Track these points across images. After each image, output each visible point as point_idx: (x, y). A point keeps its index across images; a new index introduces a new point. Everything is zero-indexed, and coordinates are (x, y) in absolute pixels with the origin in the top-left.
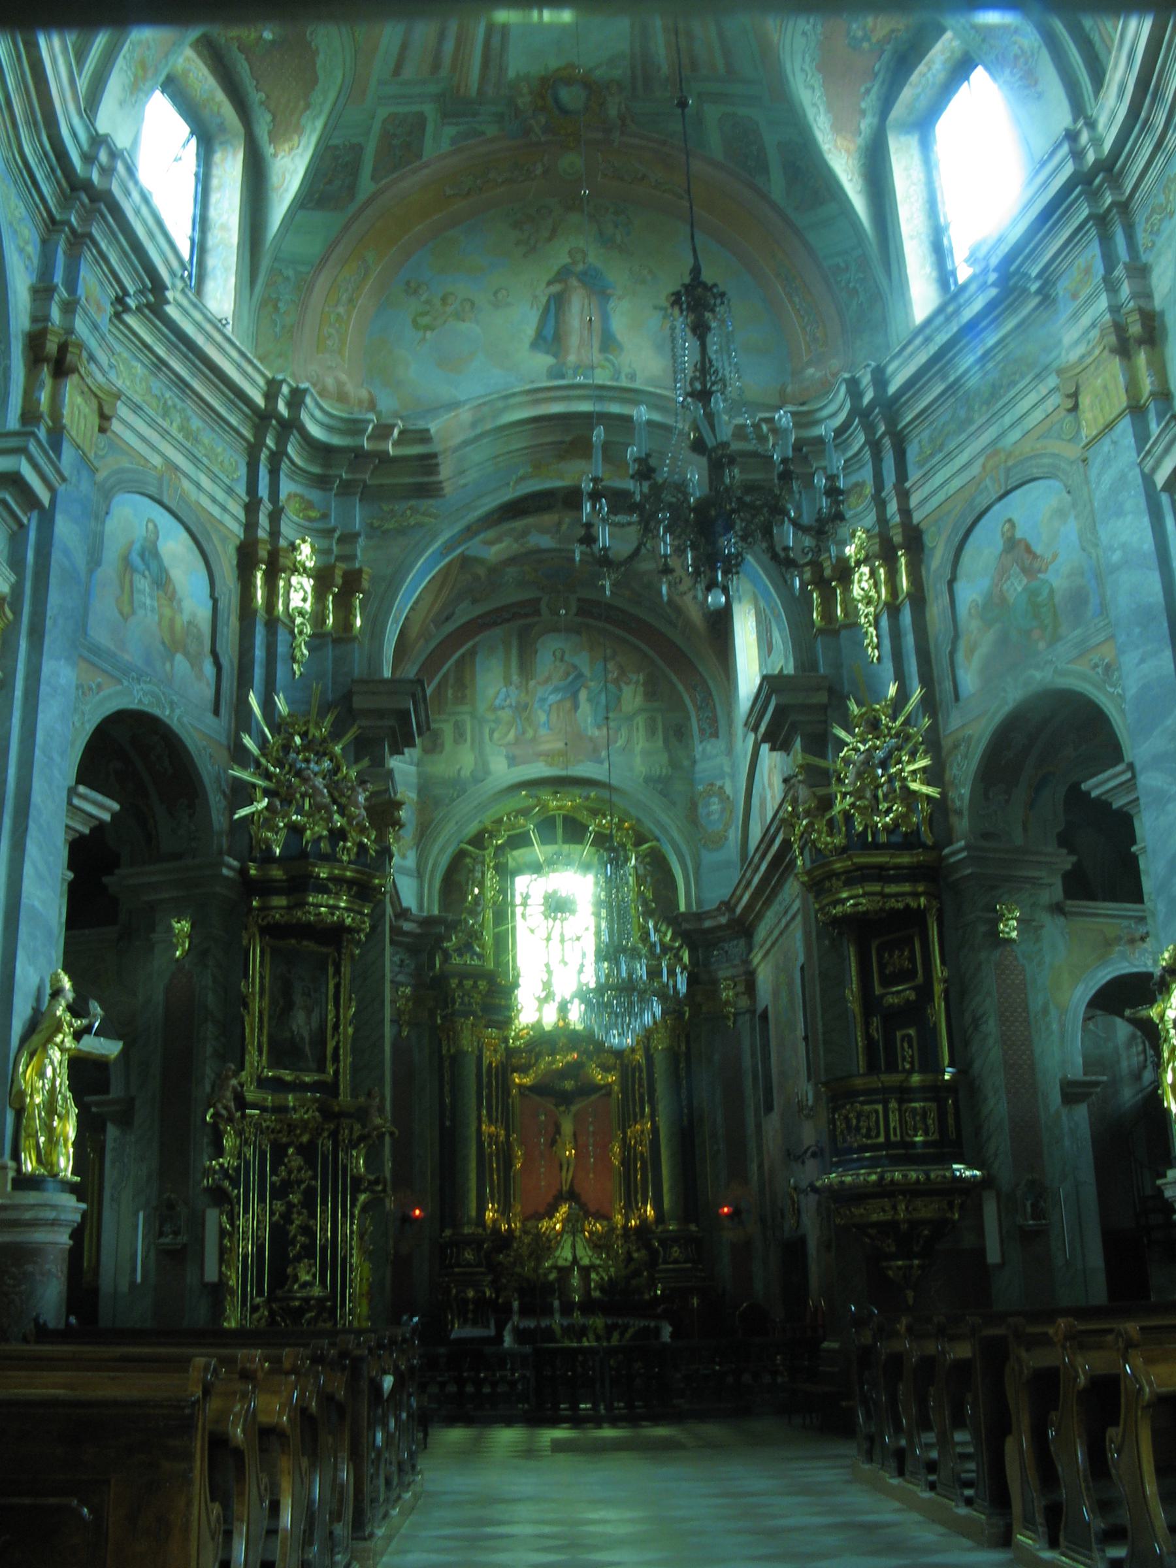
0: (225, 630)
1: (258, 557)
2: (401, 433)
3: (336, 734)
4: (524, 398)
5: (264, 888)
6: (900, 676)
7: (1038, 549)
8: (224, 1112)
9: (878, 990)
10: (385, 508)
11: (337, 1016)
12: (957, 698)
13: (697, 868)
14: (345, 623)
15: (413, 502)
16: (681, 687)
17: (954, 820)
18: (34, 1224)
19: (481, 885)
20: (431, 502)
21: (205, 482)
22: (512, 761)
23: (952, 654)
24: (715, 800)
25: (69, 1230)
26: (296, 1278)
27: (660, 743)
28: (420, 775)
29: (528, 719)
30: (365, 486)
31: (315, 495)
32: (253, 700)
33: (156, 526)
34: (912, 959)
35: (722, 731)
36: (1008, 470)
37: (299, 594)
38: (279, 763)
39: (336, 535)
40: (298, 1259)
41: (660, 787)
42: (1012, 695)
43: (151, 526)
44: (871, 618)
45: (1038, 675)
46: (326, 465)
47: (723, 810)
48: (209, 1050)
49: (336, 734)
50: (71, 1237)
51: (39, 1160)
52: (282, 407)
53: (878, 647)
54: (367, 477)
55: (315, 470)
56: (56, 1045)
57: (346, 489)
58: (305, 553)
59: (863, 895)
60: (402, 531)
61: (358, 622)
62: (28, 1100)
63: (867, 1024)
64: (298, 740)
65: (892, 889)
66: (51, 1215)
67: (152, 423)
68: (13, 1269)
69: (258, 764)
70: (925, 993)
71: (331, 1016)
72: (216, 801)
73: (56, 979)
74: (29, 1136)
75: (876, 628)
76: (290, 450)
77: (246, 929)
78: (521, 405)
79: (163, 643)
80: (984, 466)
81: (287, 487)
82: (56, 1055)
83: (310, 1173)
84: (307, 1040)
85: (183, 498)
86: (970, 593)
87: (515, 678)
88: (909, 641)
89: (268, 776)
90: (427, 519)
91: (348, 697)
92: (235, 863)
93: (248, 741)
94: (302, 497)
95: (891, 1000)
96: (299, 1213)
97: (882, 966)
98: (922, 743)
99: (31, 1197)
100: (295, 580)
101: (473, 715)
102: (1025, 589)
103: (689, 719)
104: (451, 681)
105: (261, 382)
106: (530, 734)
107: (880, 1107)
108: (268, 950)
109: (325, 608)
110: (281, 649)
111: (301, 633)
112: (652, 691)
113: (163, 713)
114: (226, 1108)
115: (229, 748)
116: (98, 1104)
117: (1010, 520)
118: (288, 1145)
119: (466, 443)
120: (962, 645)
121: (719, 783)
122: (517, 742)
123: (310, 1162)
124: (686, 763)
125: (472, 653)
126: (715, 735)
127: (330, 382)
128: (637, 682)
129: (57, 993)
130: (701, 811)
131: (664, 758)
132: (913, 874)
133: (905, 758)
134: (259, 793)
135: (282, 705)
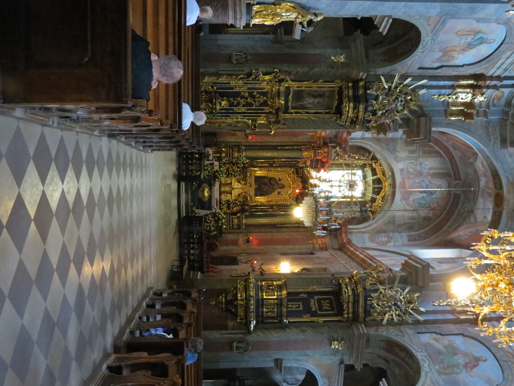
1: (479, 81)
5: (355, 88)
6: (427, 312)
7: (475, 370)
8: (278, 75)
9: (316, 298)
10: (498, 128)
11: (310, 113)
12: (419, 333)
13: (363, 232)
14: (452, 114)
15: (499, 138)
16: (426, 229)
17: (374, 328)
18: (235, 11)
19: (359, 159)
20: (499, 145)
22: (402, 170)
23: (436, 333)
24: (386, 239)
25: (233, 24)
26: (223, 101)
27: (407, 221)
28: (397, 138)
29: (417, 176)
30: (506, 120)
31: (503, 101)
32: (424, 81)
33: (492, 42)
34: (326, 310)
35: (410, 243)
36: (507, 362)
37: (464, 96)
38: (401, 92)
39: (487, 110)
40: (229, 101)
41: (392, 220)
42: (420, 355)
43: (492, 41)
44: (450, 303)
45: (426, 365)
47: (383, 242)
48: (299, 70)
49: (411, 111)
50: (231, 24)
51: (257, 12)
53: (439, 305)
56: (298, 16)
58: (480, 99)
59: (349, 295)
60: (488, 134)
61: (453, 119)
62: (278, 7)
63: (304, 293)
64: (409, 98)
65: (350, 305)
68: (219, 5)
69: (400, 84)
70: (314, 314)
71: (312, 111)
72: (386, 70)
73: (321, 14)
74: (265, 8)
75: (446, 305)
77: (341, 81)
79: (446, 48)
80: (508, 352)
81: (506, 91)
82: (294, 15)
83: (258, 105)
85: (504, 52)
86: (458, 341)
87: (431, 171)
88: (440, 317)
89: (396, 88)
90: (492, 143)
91: (424, 115)
92: (364, 77)
93: (409, 80)
94: (503, 96)
95: (312, 301)
96: (244, 101)
97: (324, 299)
98: (402, 319)
99: (244, 10)
101: (419, 157)
102: (459, 363)
103: (416, 231)
104: (431, 149)
106: (411, 176)
107: (275, 297)
108: (334, 89)
109: (459, 106)
110: (443, 91)
111: (449, 98)
112: (427, 219)
113: (420, 49)
114: (279, 76)
116: (281, 31)
117: (486, 360)
118: (267, 97)
120: (439, 337)
121: (392, 241)
122: (409, 172)
123: (261, 105)
124: (400, 230)
125: (441, 156)
126: (409, 240)
128: (429, 214)
129: (316, 15)
130: (383, 234)
131: (402, 222)
132: (355, 312)
133: (397, 312)
134: (390, 84)
135: (422, 92)
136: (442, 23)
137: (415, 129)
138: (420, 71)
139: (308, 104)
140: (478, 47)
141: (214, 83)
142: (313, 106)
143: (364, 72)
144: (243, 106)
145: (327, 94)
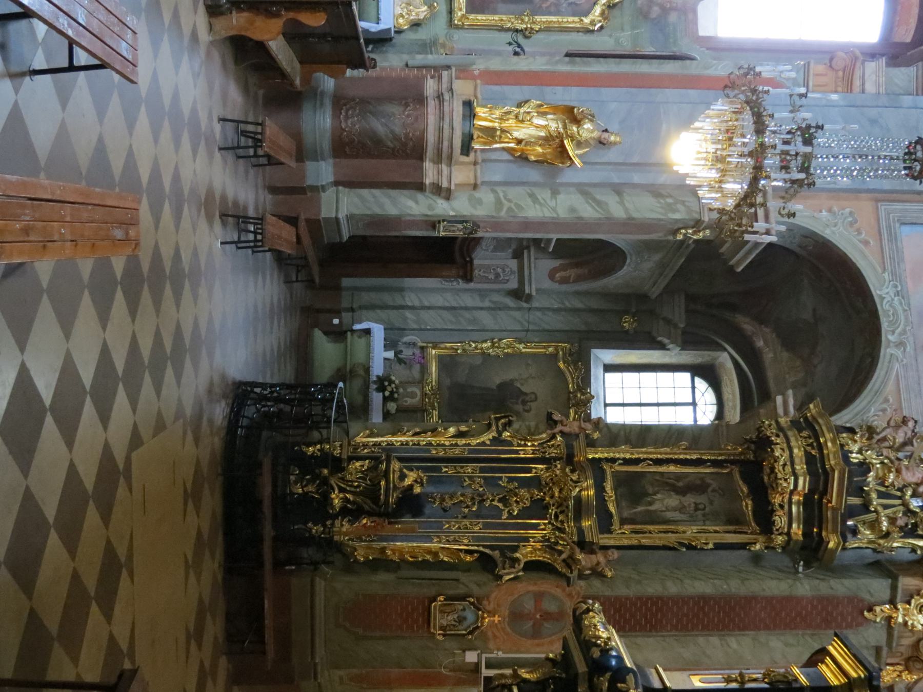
84: (651, 508)
113: (889, 336)
139: (667, 510)
142: (684, 517)
145: (714, 485)
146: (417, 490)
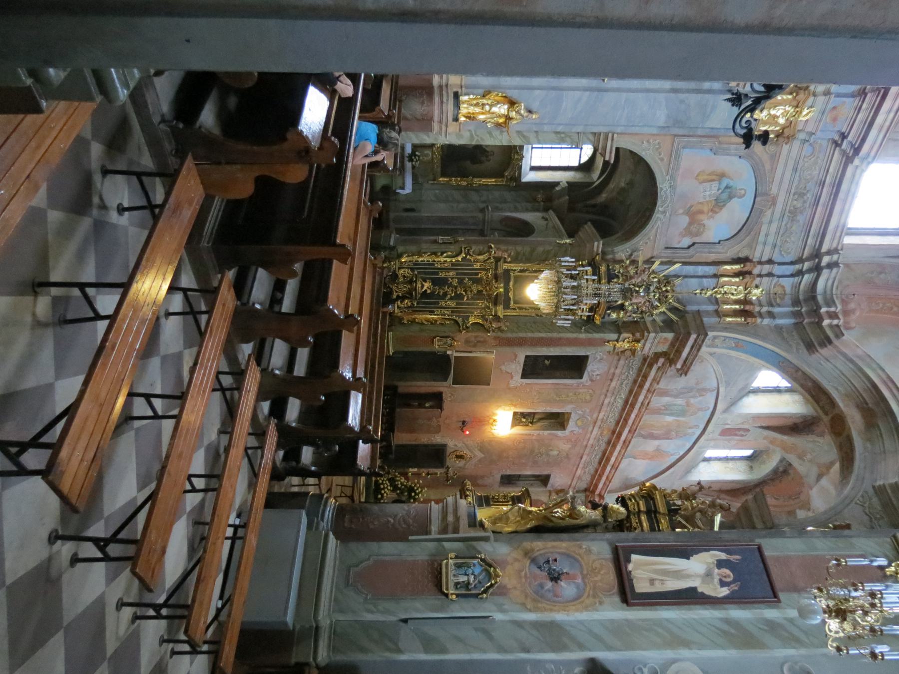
0: (706, 250)
1: (744, 267)
2: (837, 326)
3: (673, 309)
4: (884, 377)
10: (794, 333)
18: (441, 95)
20: (805, 350)
21: (774, 226)
30: (801, 323)
31: (788, 300)
32: (677, 265)
33: (744, 195)
37: (733, 289)
39: (771, 309)
43: (743, 192)
46: (806, 300)
52: (826, 260)
54: (806, 321)
55: (801, 297)
57: (797, 314)
64: (664, 289)
66: (445, 100)
67: (791, 182)
76: (806, 276)
78: (879, 376)
79: (691, 206)
81: (787, 283)
85: (761, 212)
100: (741, 288)
105: (834, 245)
109: (732, 304)
113: (659, 208)
115: (652, 257)
119: (845, 355)
127: (852, 306)
135: (677, 282)
136: (676, 155)
137: (682, 330)
138: (669, 251)
140: (728, 204)
141: (415, 264)
143: (598, 241)
144: (451, 298)
146: (429, 291)
